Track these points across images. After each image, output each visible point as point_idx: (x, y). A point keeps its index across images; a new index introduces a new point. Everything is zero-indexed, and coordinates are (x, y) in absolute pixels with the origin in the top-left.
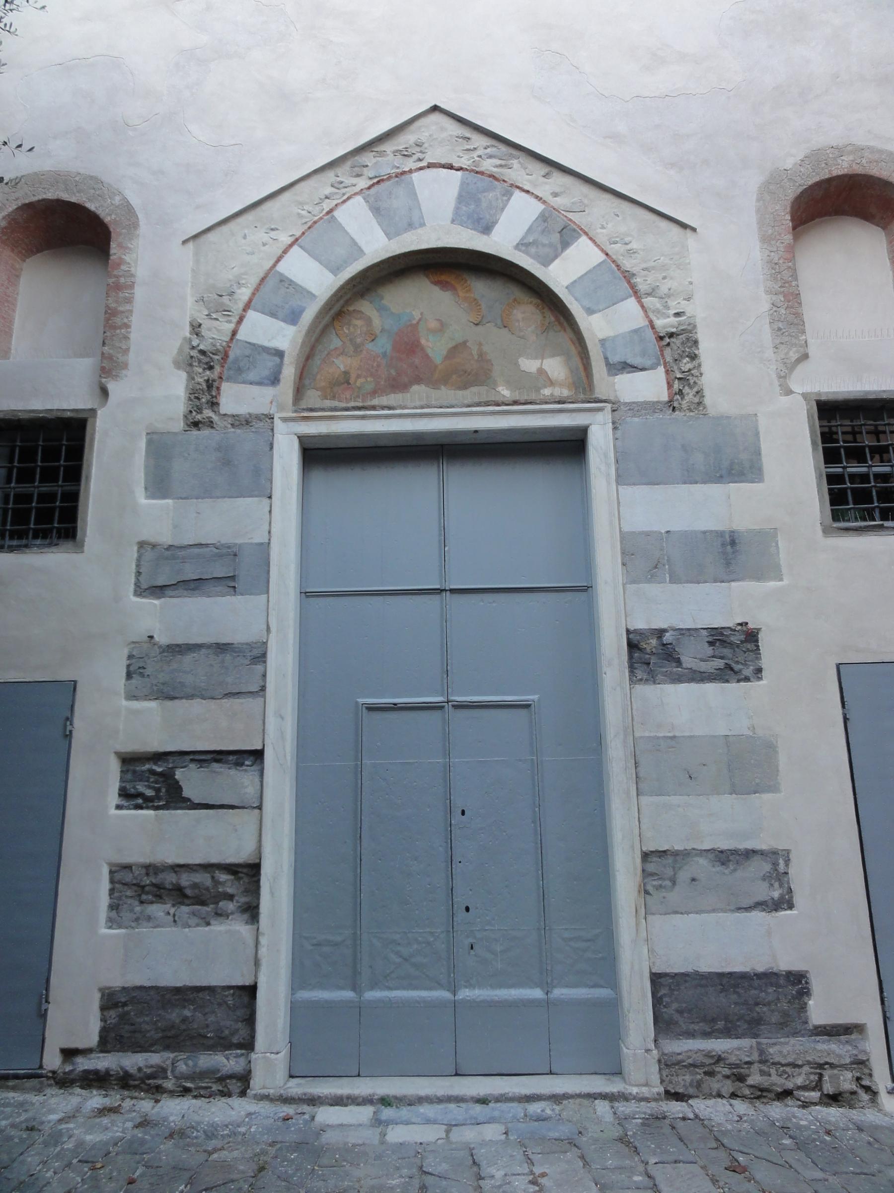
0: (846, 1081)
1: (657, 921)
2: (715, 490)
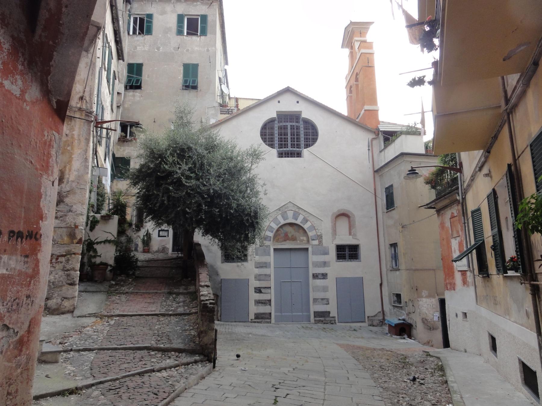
0: (333, 322)
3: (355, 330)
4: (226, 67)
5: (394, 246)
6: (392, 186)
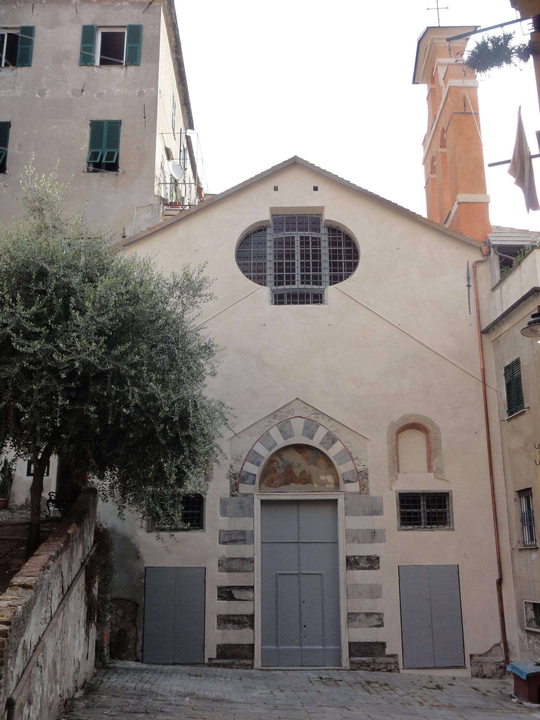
0: (393, 667)
1: (350, 629)
2: (370, 517)
3: (438, 687)
4: (189, 132)
5: (525, 494)
6: (517, 362)
